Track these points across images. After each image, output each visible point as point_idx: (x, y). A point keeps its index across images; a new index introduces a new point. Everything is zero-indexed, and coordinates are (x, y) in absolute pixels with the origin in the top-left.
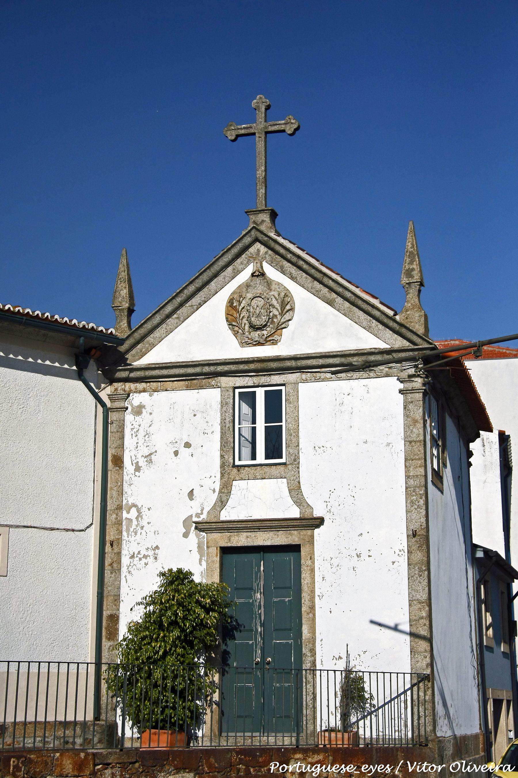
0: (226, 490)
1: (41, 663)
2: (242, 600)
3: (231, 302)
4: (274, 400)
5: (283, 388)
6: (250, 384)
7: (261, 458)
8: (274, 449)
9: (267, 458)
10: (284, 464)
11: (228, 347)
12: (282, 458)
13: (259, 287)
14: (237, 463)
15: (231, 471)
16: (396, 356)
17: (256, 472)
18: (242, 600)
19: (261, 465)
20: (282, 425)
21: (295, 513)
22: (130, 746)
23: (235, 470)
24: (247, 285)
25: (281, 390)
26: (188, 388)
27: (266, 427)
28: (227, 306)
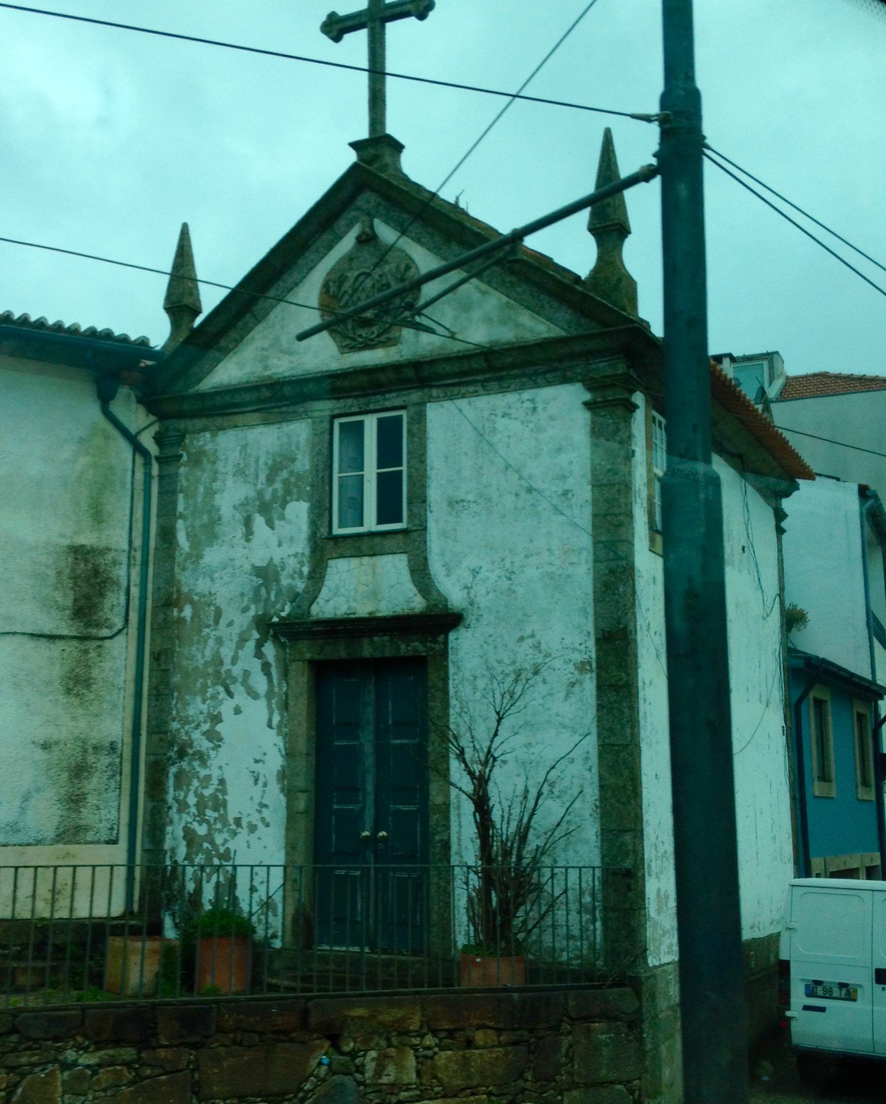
0: (317, 575)
1: (115, 868)
2: (398, 741)
3: (326, 285)
4: (389, 435)
5: (403, 413)
6: (355, 409)
7: (371, 523)
8: (388, 509)
9: (381, 520)
10: (404, 532)
11: (323, 355)
12: (400, 520)
13: (368, 258)
14: (337, 531)
15: (325, 547)
16: (577, 348)
17: (363, 546)
18: (398, 741)
19: (371, 535)
20: (401, 472)
21: (418, 604)
22: (47, 914)
23: (331, 543)
24: (350, 258)
25: (401, 416)
26: (267, 423)
27: (379, 474)
28: (321, 294)
